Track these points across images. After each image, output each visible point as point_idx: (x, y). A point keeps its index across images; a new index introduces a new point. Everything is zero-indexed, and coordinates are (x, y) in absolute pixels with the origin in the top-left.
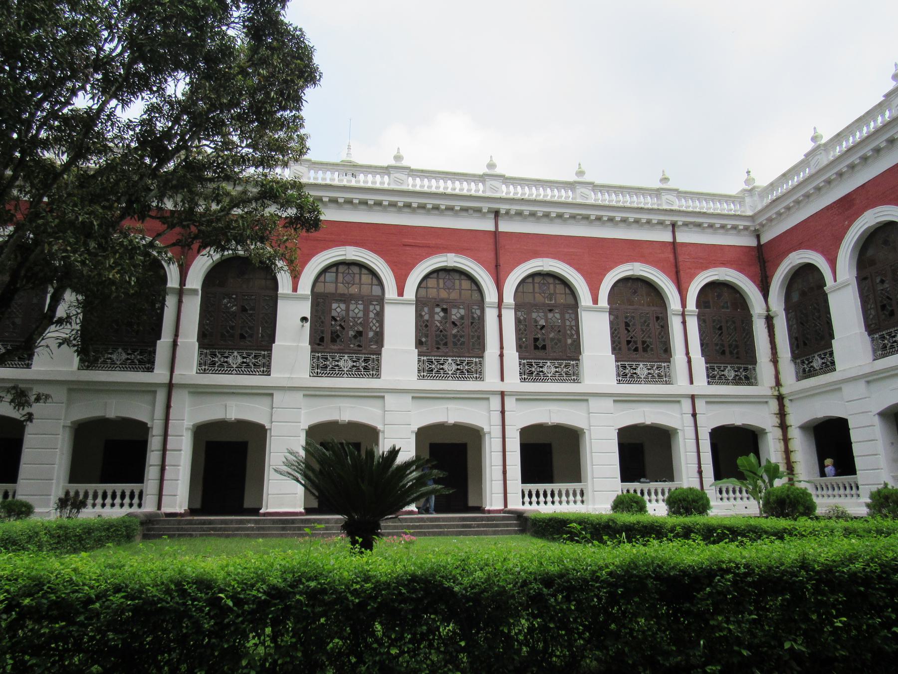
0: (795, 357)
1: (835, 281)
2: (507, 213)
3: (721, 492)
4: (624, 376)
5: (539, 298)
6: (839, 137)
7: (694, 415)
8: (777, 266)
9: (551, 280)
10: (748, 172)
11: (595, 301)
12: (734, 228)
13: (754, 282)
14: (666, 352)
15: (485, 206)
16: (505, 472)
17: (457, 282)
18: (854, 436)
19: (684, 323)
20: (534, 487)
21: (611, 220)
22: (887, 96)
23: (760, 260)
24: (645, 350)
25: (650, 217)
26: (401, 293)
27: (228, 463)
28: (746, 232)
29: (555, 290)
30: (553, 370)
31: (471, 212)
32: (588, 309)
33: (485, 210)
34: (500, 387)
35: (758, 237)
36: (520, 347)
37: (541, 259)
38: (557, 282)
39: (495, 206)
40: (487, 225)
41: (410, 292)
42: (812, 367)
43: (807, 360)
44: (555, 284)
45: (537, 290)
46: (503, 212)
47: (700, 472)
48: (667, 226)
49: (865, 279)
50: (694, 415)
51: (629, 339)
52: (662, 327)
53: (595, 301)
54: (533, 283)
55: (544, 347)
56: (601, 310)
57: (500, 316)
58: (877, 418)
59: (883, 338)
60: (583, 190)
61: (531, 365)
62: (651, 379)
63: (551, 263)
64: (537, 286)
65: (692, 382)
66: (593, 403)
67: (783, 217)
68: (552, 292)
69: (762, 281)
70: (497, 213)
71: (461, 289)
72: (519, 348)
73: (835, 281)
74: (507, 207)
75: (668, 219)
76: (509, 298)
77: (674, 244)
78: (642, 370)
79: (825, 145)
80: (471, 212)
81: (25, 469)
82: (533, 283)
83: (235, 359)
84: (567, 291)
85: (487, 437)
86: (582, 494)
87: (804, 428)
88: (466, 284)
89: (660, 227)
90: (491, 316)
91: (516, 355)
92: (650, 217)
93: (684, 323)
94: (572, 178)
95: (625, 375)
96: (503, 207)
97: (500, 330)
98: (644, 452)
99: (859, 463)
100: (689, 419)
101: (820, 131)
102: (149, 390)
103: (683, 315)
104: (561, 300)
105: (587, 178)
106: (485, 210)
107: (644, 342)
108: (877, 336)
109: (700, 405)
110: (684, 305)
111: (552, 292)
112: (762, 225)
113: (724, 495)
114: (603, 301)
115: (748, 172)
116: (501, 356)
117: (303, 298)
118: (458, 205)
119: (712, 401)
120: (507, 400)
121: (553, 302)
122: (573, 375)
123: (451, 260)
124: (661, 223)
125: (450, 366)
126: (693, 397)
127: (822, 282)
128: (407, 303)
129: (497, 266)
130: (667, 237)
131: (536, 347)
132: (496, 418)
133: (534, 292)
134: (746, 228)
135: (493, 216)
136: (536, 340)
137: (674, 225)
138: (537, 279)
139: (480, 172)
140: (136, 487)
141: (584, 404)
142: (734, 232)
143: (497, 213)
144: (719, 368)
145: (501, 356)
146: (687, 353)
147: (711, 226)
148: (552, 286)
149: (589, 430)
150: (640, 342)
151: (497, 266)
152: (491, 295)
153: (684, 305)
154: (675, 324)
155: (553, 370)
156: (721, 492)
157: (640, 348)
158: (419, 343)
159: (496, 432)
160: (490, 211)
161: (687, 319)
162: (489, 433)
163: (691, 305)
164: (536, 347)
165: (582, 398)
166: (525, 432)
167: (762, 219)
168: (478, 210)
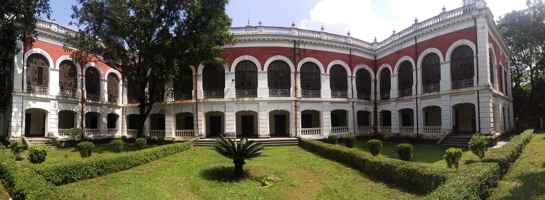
4: (333, 95)
5: (308, 70)
7: (353, 107)
11: (326, 72)
14: (346, 89)
19: (352, 80)
20: (305, 129)
21: (331, 46)
27: (215, 122)
32: (323, 74)
34: (295, 99)
50: (353, 107)
53: (326, 72)
55: (309, 86)
56: (327, 75)
62: (342, 97)
78: (339, 94)
81: (166, 127)
86: (320, 131)
93: (352, 80)
94: (320, 30)
97: (296, 82)
98: (338, 118)
100: (351, 108)
103: (352, 77)
105: (324, 31)
109: (355, 104)
110: (352, 74)
114: (328, 72)
119: (358, 103)
120: (297, 103)
122: (319, 95)
126: (353, 102)
132: (294, 108)
136: (307, 84)
140: (192, 131)
141: (321, 104)
150: (339, 85)
153: (352, 74)
154: (349, 79)
164: (307, 86)
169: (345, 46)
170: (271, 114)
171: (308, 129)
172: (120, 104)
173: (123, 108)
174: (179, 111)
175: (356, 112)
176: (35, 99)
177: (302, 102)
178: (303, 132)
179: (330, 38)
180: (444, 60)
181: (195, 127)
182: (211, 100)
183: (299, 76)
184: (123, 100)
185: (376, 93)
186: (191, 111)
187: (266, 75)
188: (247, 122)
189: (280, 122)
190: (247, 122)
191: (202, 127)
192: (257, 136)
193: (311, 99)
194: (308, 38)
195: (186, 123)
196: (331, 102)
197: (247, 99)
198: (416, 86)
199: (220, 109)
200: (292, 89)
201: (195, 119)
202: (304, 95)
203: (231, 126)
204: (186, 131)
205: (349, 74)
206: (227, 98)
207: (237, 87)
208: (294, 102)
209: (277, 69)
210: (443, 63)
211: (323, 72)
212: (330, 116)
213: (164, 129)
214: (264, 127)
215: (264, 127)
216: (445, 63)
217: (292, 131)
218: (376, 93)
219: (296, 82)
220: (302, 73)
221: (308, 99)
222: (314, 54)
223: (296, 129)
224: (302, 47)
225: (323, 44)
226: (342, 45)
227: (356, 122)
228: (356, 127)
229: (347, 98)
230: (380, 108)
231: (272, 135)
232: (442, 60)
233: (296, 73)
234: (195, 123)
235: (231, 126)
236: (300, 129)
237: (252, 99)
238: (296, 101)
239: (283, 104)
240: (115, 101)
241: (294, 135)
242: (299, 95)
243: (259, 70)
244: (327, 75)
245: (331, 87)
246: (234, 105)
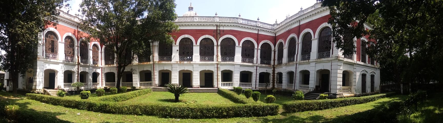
4: (243, 61)
26: (196, 44)
27: (165, 77)
34: (217, 62)
41: (198, 43)
72: (221, 55)
76: (219, 43)
83: (165, 58)
88: (210, 41)
90: (215, 48)
97: (217, 51)
102: (151, 65)
114: (241, 45)
117: (177, 46)
118: (208, 24)
122: (233, 60)
123: (207, 36)
125: (207, 58)
128: (198, 46)
132: (216, 69)
150: (248, 54)
158: (200, 54)
159: (216, 72)
165: (234, 65)
166: (222, 71)
168: (213, 25)
170: (201, 72)
172: (99, 65)
173: (102, 68)
174: (142, 70)
176: (50, 63)
177: (221, 65)
181: (152, 79)
182: (163, 62)
183: (219, 48)
184: (101, 63)
185: (274, 60)
186: (150, 69)
187: (198, 48)
188: (186, 77)
189: (207, 79)
190: (186, 77)
191: (156, 80)
192: (191, 87)
193: (227, 62)
195: (146, 77)
196: (241, 66)
197: (186, 62)
199: (168, 68)
200: (215, 57)
201: (152, 74)
202: (224, 60)
203: (175, 80)
204: (145, 82)
206: (173, 61)
207: (180, 55)
208: (217, 65)
209: (205, 43)
211: (237, 44)
213: (132, 81)
214: (196, 81)
215: (196, 81)
217: (215, 84)
218: (274, 60)
219: (217, 51)
220: (221, 45)
221: (225, 63)
223: (218, 83)
224: (221, 28)
229: (253, 63)
230: (277, 71)
231: (201, 87)
233: (217, 46)
234: (152, 77)
235: (175, 80)
236: (220, 82)
237: (189, 62)
238: (217, 64)
239: (209, 66)
240: (97, 64)
241: (216, 86)
242: (220, 59)
243: (194, 44)
245: (242, 55)
246: (178, 66)
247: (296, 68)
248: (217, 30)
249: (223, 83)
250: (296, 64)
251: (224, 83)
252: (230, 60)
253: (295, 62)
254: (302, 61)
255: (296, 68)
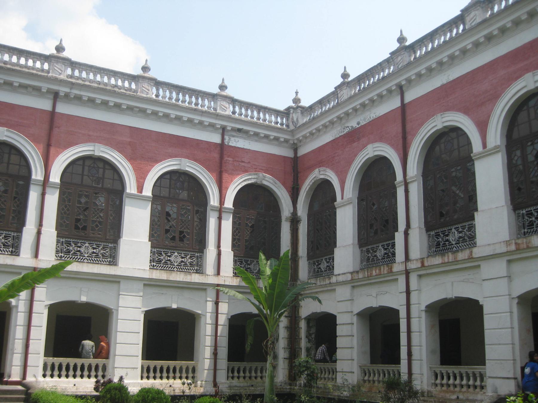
0: (309, 257)
1: (342, 198)
2: (67, 95)
3: (233, 372)
4: (156, 262)
5: (87, 181)
6: (360, 79)
8: (306, 177)
9: (101, 165)
10: (297, 93)
11: (140, 188)
12: (277, 139)
13: (286, 189)
14: (201, 245)
15: (45, 86)
16: (27, 346)
17: (6, 156)
18: (340, 330)
19: (220, 219)
22: (392, 54)
23: (294, 169)
24: (181, 240)
25: (203, 119)
28: (285, 144)
29: (103, 175)
30: (91, 250)
31: (30, 89)
32: (131, 196)
33: (44, 90)
35: (296, 151)
36: (60, 226)
37: (92, 144)
38: (107, 167)
39: (55, 87)
40: (45, 105)
42: (320, 268)
43: (318, 261)
44: (104, 169)
45: (86, 173)
46: (62, 94)
47: (215, 354)
48: (217, 129)
49: (362, 200)
51: (167, 228)
52: (200, 219)
54: (83, 166)
55: (84, 228)
57: (43, 195)
58: (355, 319)
59: (368, 251)
60: (146, 85)
61: (69, 244)
63: (102, 149)
64: (86, 168)
65: (218, 273)
66: (123, 285)
67: (315, 136)
68: (101, 176)
69: (293, 188)
70: (56, 96)
71: (8, 164)
73: (342, 198)
74: (67, 90)
75: (219, 123)
76: (55, 177)
77: (222, 147)
78: (176, 258)
79: (349, 83)
80: (30, 89)
82: (83, 166)
84: (116, 177)
85: (14, 311)
86: (104, 368)
87: (309, 319)
88: (15, 158)
89: (211, 129)
91: (55, 233)
92: (203, 119)
93: (220, 219)
95: (160, 261)
96: (63, 90)
99: (340, 354)
101: (348, 71)
103: (220, 211)
104: (108, 184)
106: (44, 90)
107: (181, 232)
108: (364, 249)
111: (101, 176)
112: (298, 139)
113: (236, 374)
114: (148, 192)
115: (297, 93)
116: (39, 233)
121: (100, 186)
124: (212, 126)
127: (335, 200)
129: (48, 146)
130: (216, 138)
131: (77, 228)
133: (83, 175)
134: (286, 141)
135: (52, 97)
136: (78, 220)
137: (224, 129)
138: (88, 163)
139: (47, 53)
141: (115, 286)
142: (276, 143)
143: (56, 96)
144: (246, 262)
145: (39, 233)
146: (219, 246)
147: (256, 134)
148: (101, 171)
149: (117, 310)
151: (48, 146)
152: (37, 175)
155: (91, 250)
156: (233, 372)
157: (177, 238)
160: (49, 91)
161: (224, 215)
162: (17, 307)
163: (229, 203)
164: (77, 228)
167: (299, 135)
168: (38, 89)
169: (207, 120)
171: (64, 361)
175: (223, 320)
178: (50, 370)
179: (165, 95)
180: (484, 146)
194: (103, 91)
196: (149, 284)
198: (406, 234)
205: (214, 201)
210: (481, 156)
211: (131, 187)
212: (140, 327)
216: (487, 153)
222: (108, 133)
225: (143, 111)
226: (197, 118)
227: (223, 352)
228: (223, 363)
232: (477, 146)
241: (16, 376)
244: (145, 198)
247: (408, 292)
248: (53, 114)
249: (51, 360)
250: (407, 273)
251: (57, 360)
252: (94, 259)
253: (398, 267)
254: (438, 260)
255: (408, 292)
